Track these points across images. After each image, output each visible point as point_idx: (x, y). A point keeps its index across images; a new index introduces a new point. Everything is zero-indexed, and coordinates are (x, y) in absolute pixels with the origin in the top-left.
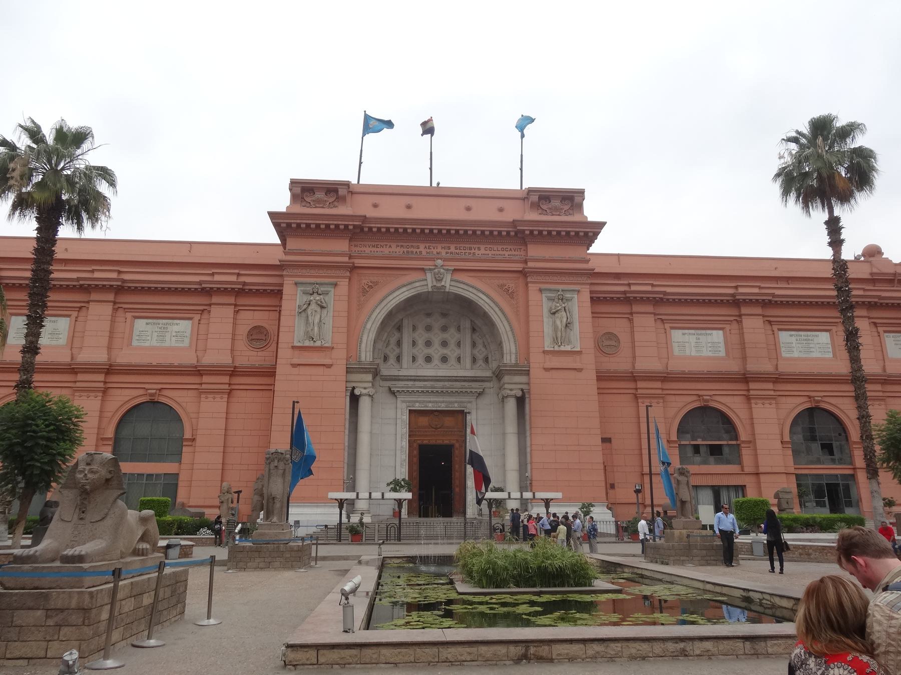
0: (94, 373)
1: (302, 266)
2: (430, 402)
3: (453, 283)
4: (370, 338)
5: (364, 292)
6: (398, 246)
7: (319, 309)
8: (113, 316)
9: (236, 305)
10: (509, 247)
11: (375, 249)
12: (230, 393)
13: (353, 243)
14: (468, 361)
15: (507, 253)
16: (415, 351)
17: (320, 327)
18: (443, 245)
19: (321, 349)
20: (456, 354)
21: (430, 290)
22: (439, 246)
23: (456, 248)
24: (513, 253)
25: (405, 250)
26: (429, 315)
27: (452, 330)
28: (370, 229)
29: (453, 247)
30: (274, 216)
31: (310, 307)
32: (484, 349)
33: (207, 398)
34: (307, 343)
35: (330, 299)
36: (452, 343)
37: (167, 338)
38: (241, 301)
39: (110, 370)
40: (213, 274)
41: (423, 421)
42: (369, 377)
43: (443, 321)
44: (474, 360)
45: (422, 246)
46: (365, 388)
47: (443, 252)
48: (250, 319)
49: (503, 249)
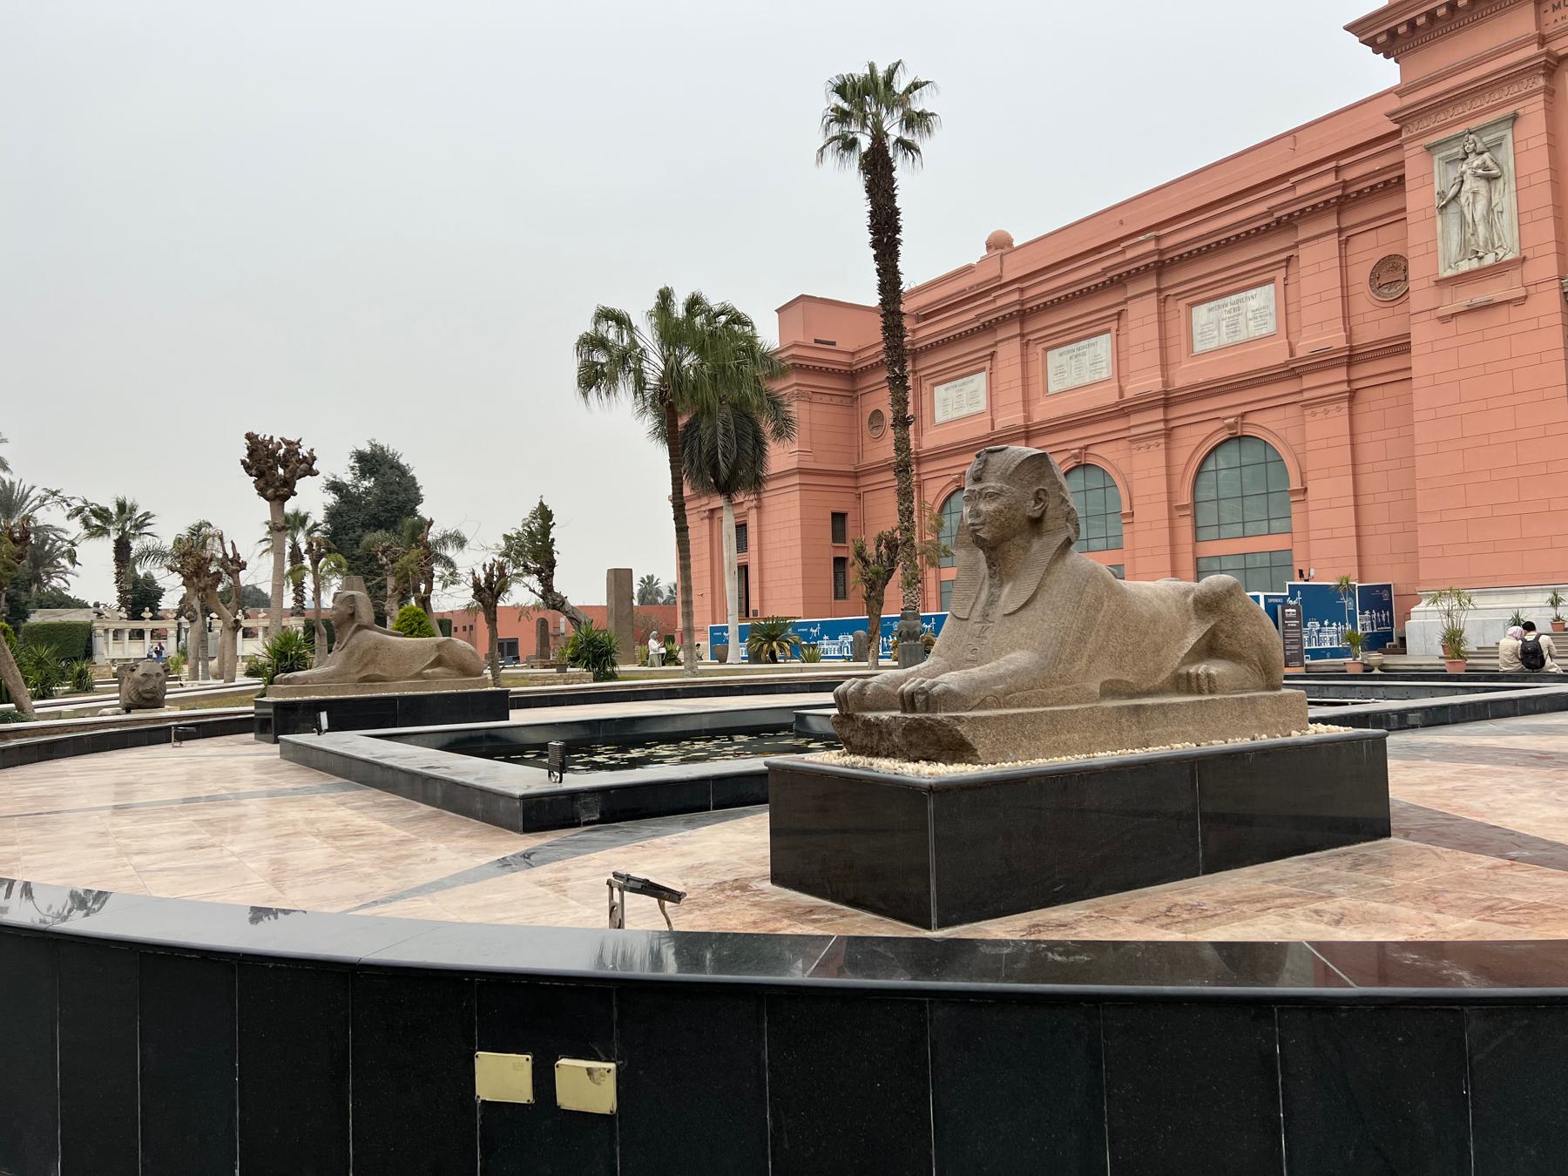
0: (1254, 386)
1: (1435, 107)
7: (1482, 186)
8: (1161, 315)
9: (1340, 231)
12: (1352, 396)
17: (1490, 225)
19: (1499, 268)
31: (1466, 187)
33: (1314, 414)
34: (1465, 266)
35: (1507, 155)
37: (1242, 326)
38: (1351, 218)
39: (1167, 400)
40: (1293, 187)
48: (1368, 250)
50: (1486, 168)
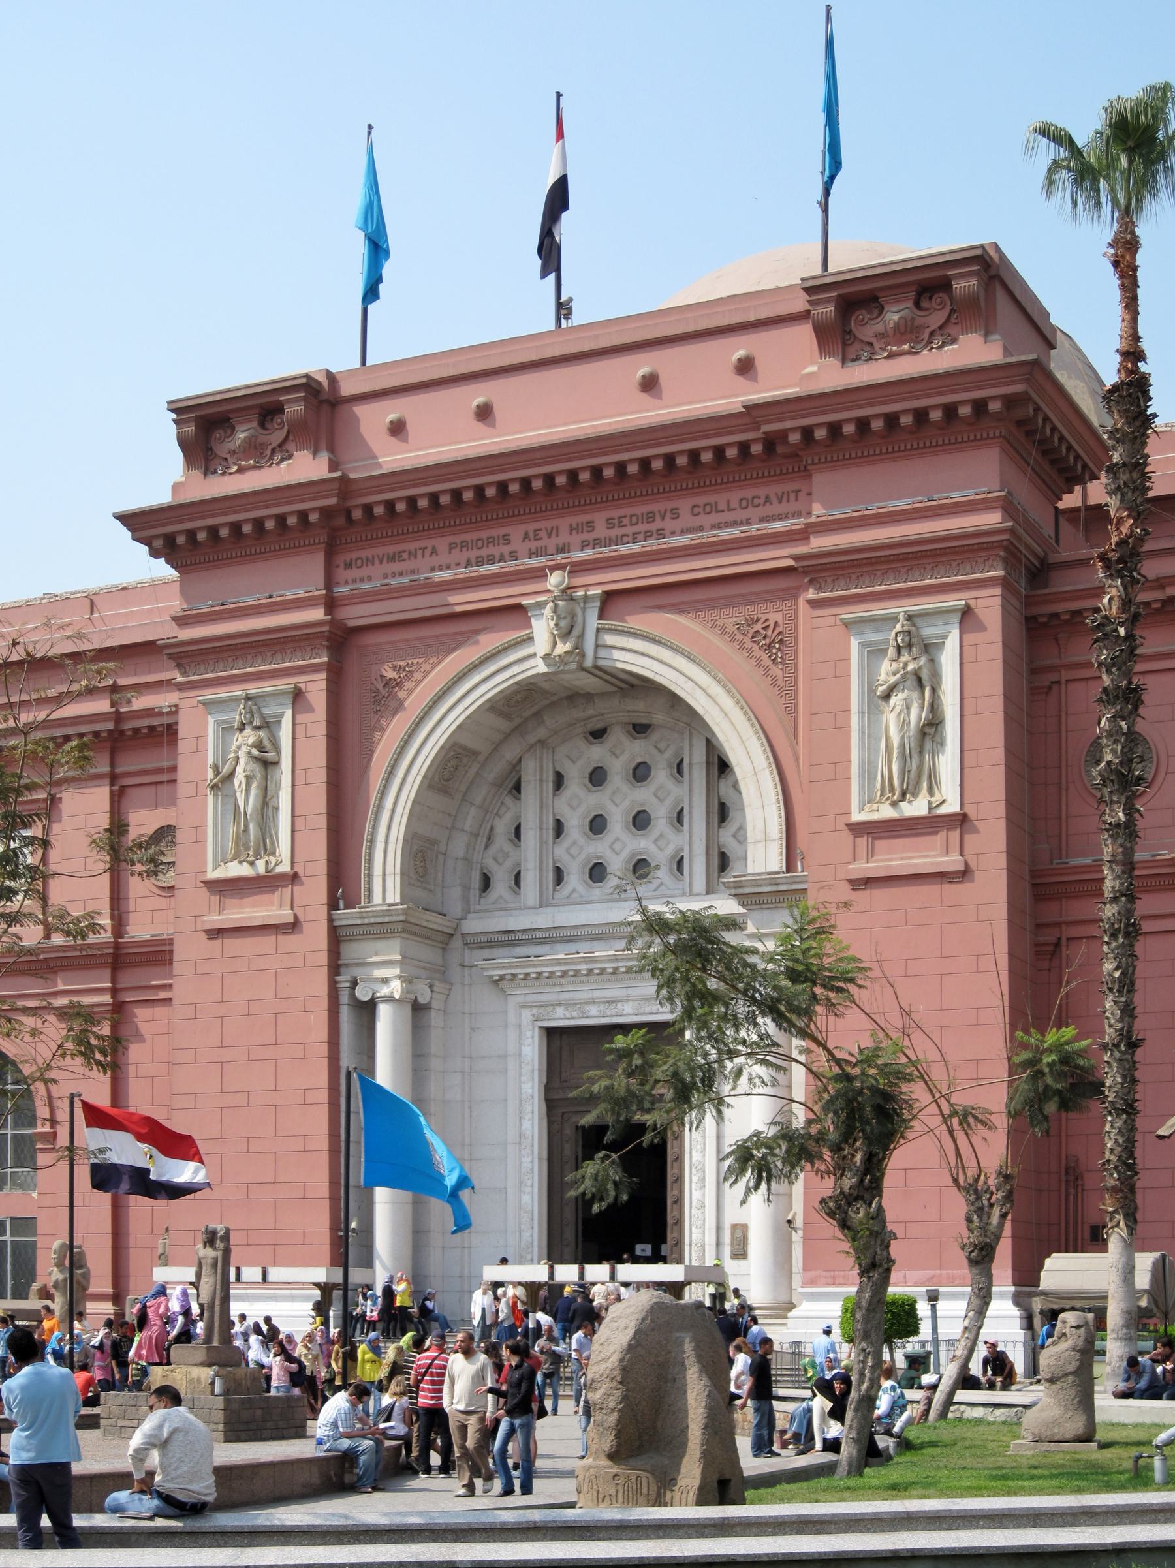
6: (452, 547)
9: (113, 778)
10: (761, 492)
11: (396, 567)
13: (340, 560)
14: (698, 867)
18: (575, 520)
20: (670, 850)
21: (542, 668)
22: (564, 523)
23: (610, 523)
24: (776, 508)
25: (473, 554)
26: (598, 734)
29: (599, 519)
30: (138, 523)
45: (516, 532)
47: (576, 539)
49: (746, 503)
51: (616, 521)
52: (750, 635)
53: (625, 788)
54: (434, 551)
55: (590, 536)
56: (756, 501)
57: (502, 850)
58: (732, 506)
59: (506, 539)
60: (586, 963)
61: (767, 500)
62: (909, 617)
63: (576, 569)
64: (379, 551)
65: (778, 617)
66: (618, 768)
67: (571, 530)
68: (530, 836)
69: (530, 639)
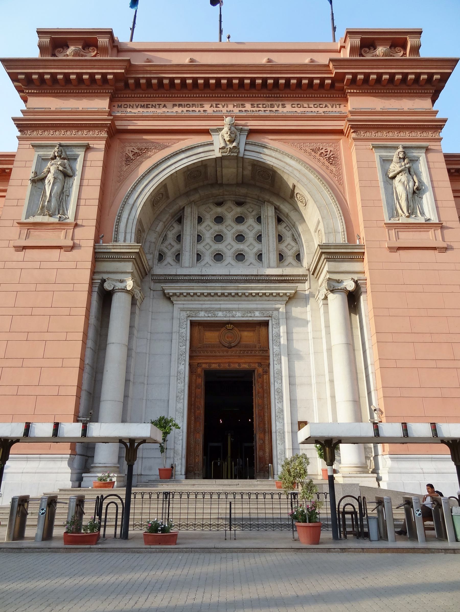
2: (220, 310)
3: (248, 147)
4: (131, 217)
5: (128, 160)
6: (174, 105)
7: (61, 177)
10: (324, 104)
11: (145, 110)
13: (116, 104)
15: (321, 110)
16: (200, 247)
20: (255, 250)
21: (217, 154)
23: (253, 106)
24: (330, 109)
26: (219, 204)
27: (251, 221)
28: (137, 80)
32: (293, 244)
36: (250, 237)
41: (211, 337)
42: (129, 267)
43: (238, 210)
44: (281, 257)
46: (122, 281)
47: (236, 110)
50: (65, 168)
51: (256, 106)
52: (319, 153)
53: (233, 224)
54: (165, 106)
55: (243, 109)
56: (321, 106)
57: (170, 244)
58: (310, 106)
59: (202, 106)
60: (221, 289)
61: (326, 106)
62: (404, 148)
63: (238, 118)
64: (137, 103)
65: (332, 149)
66: (230, 217)
67: (234, 106)
68: (188, 239)
69: (212, 144)
